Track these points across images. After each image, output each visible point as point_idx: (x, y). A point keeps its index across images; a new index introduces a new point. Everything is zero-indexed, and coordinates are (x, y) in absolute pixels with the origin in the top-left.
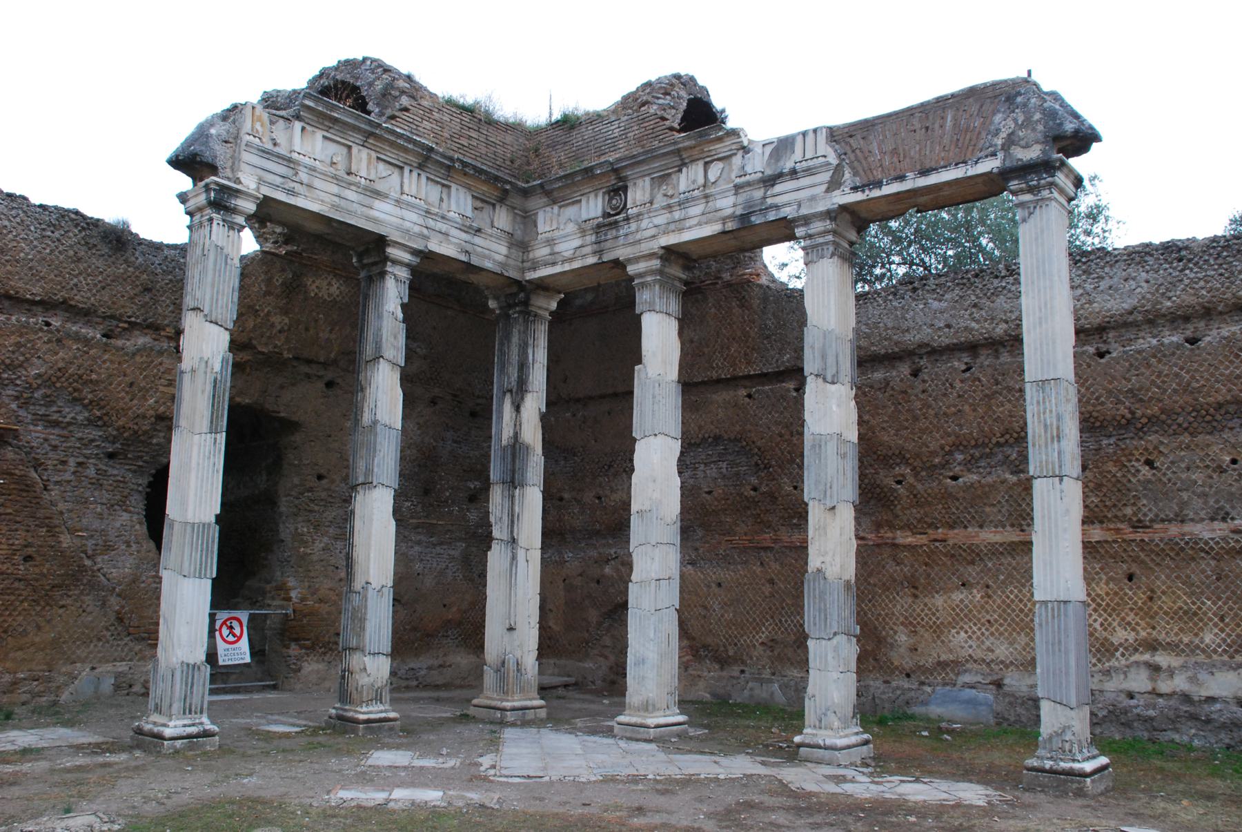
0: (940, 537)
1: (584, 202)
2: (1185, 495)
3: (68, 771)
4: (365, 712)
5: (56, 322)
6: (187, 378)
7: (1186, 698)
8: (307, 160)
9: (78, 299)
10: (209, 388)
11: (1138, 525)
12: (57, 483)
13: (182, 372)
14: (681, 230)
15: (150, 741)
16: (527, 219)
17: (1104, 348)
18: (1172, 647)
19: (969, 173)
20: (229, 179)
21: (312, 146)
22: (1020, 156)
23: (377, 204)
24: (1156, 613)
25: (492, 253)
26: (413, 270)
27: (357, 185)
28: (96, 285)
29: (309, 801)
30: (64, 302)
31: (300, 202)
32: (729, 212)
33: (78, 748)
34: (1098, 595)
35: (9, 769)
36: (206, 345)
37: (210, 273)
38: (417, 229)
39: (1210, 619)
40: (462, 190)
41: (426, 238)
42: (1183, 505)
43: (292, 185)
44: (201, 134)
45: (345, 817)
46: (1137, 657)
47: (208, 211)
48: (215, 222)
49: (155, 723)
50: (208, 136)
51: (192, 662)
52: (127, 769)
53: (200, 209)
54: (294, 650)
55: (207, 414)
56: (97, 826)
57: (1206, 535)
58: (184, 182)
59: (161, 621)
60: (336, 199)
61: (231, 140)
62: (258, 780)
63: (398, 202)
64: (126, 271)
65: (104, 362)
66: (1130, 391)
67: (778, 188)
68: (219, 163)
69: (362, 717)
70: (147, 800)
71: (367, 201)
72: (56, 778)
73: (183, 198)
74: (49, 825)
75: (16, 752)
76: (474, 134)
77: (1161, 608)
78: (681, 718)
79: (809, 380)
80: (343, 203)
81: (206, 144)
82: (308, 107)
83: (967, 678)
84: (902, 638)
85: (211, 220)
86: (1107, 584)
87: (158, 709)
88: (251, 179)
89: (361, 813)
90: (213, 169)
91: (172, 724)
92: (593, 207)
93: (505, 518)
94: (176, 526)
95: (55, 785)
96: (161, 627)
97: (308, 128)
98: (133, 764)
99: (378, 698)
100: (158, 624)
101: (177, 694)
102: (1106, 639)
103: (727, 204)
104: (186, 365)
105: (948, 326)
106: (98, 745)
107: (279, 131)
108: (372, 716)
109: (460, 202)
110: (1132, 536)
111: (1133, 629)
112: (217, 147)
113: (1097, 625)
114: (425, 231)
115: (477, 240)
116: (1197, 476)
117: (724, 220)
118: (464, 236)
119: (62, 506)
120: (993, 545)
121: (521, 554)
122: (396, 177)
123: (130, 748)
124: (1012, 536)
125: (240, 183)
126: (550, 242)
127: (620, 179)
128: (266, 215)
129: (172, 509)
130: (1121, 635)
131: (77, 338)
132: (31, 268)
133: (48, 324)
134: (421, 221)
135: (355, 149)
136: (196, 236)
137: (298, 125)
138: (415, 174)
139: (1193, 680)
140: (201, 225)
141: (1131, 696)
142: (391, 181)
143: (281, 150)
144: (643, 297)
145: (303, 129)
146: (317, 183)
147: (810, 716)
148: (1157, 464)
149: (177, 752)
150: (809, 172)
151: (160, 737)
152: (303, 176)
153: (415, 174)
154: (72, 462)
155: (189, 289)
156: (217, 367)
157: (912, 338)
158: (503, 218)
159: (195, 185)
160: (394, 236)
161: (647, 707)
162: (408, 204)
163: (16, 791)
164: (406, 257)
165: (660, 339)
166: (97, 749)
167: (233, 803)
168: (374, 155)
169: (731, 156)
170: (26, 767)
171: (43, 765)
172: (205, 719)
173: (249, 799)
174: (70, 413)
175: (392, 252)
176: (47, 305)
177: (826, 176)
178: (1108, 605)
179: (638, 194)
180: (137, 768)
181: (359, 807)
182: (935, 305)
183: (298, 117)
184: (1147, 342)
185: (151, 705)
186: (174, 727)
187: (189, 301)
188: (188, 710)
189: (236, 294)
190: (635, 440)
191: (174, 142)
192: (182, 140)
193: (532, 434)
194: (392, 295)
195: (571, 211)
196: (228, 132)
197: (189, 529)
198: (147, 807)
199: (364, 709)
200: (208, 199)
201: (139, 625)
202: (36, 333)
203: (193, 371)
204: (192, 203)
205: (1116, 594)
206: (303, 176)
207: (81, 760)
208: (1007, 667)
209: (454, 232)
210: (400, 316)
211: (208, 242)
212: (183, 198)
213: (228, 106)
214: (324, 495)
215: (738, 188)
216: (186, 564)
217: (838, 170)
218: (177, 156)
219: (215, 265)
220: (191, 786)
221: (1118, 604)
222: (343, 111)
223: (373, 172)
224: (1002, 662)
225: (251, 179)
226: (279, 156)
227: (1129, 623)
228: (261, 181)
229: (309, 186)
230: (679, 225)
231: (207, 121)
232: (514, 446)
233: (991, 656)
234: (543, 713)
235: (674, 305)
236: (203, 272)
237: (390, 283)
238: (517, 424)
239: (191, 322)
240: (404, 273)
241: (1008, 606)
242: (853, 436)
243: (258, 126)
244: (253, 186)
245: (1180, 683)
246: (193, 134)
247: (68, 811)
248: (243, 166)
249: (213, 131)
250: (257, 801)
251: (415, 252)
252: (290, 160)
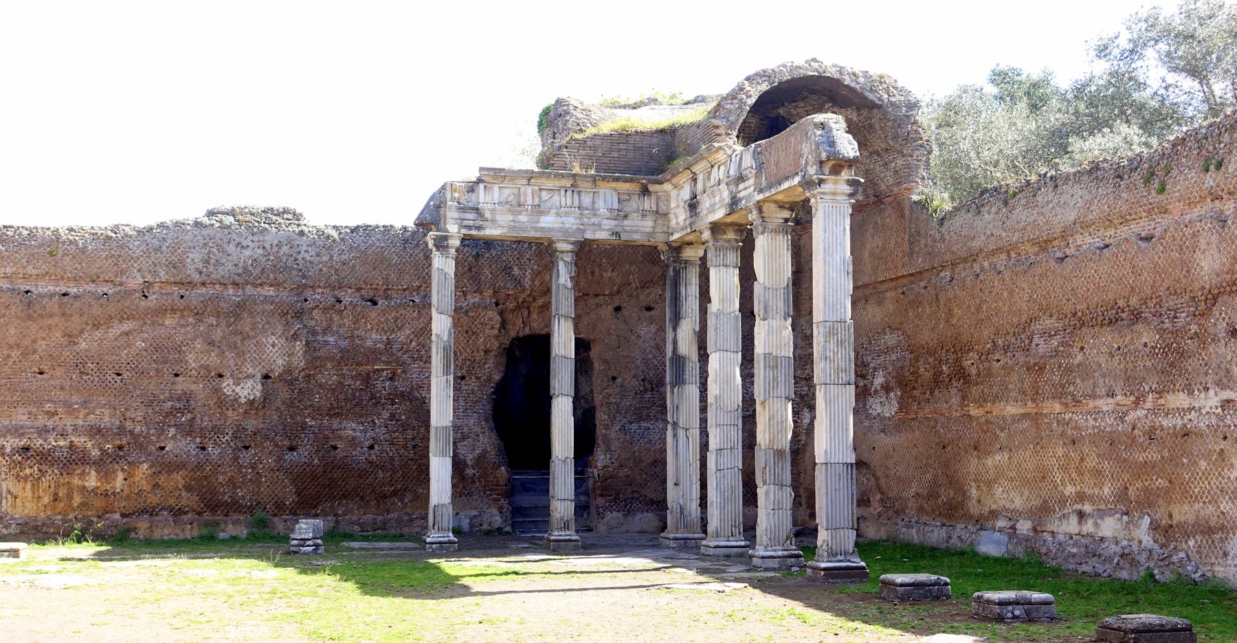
4: (556, 535)
25: (640, 229)
41: (583, 231)
71: (535, 218)
99: (566, 526)
118: (614, 222)
156: (446, 338)
164: (569, 247)
172: (451, 534)
194: (563, 276)
209: (605, 222)
210: (569, 285)
228: (461, 227)
237: (561, 265)
238: (675, 342)
240: (568, 258)
251: (574, 243)
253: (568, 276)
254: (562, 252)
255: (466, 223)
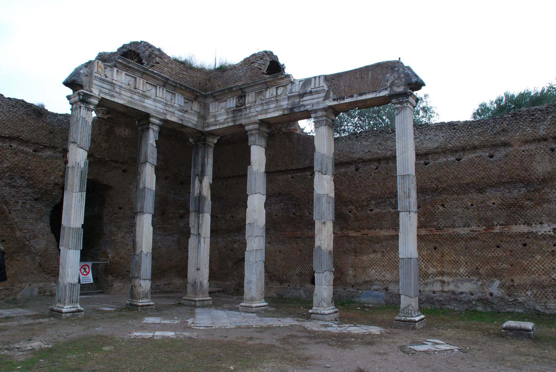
0: (365, 233)
1: (228, 101)
2: (455, 218)
3: (26, 325)
5: (14, 146)
6: (70, 171)
7: (453, 293)
8: (119, 83)
9: (23, 136)
10: (79, 174)
11: (438, 229)
12: (14, 210)
13: (68, 168)
14: (267, 113)
15: (56, 314)
16: (206, 107)
17: (427, 161)
18: (449, 274)
19: (377, 96)
20: (88, 91)
21: (121, 78)
22: (396, 90)
23: (146, 101)
24: (444, 262)
25: (192, 120)
26: (160, 127)
27: (139, 93)
28: (30, 130)
29: (123, 336)
30: (18, 137)
31: (116, 100)
32: (286, 107)
33: (28, 317)
34: (424, 255)
35: (2, 324)
36: (78, 156)
37: (80, 128)
38: (162, 111)
39: (463, 264)
40: (180, 95)
41: (165, 114)
42: (454, 221)
43: (113, 93)
44: (77, 72)
45: (138, 342)
46: (437, 278)
47: (79, 103)
48: (82, 109)
49: (58, 307)
50: (80, 73)
51: (73, 283)
52: (49, 324)
53: (76, 102)
54: (110, 278)
55: (78, 184)
56: (43, 346)
57: (462, 232)
58: (70, 92)
59: (60, 266)
60: (130, 99)
61: (89, 75)
62: (101, 329)
63: (155, 100)
64: (43, 125)
65: (34, 162)
66: (436, 178)
67: (305, 98)
68: (84, 84)
69: (140, 304)
70: (59, 336)
71: (142, 99)
72: (22, 328)
73: (69, 98)
74: (24, 345)
75: (3, 318)
76: (185, 73)
77: (446, 260)
78: (265, 304)
79: (316, 173)
80: (133, 100)
81: (79, 77)
82: (120, 62)
83: (375, 287)
84: (351, 272)
85: (80, 107)
86: (427, 251)
87: (59, 301)
88: (97, 91)
89: (143, 341)
90: (82, 87)
91: (65, 307)
92: (232, 103)
93: (196, 226)
94: (66, 229)
95: (22, 330)
96: (60, 269)
97: (120, 70)
98: (51, 322)
99: (146, 297)
100: (59, 268)
101: (67, 295)
102: (426, 272)
103: (285, 103)
104: (70, 165)
105: (370, 152)
106: (35, 315)
107: (108, 72)
108: (144, 304)
109: (179, 100)
110: (435, 233)
111: (436, 268)
112: (83, 78)
113: (423, 266)
114: (165, 111)
115: (186, 115)
116: (460, 210)
117: (284, 110)
119: (16, 220)
120: (385, 236)
121: (202, 240)
122: (154, 90)
123: (49, 317)
124: (393, 233)
125: (92, 92)
126: (215, 116)
127: (243, 92)
128: (103, 104)
129: (64, 222)
130: (431, 270)
131: (23, 152)
132: (4, 124)
133: (11, 146)
134: (163, 107)
135: (138, 79)
136: (74, 113)
137: (115, 69)
138: (161, 89)
139: (456, 286)
140: (76, 109)
141: (434, 292)
142: (152, 92)
143: (109, 79)
144: (251, 139)
145: (117, 71)
146: (123, 92)
147: (315, 302)
148: (445, 206)
149: (68, 318)
150: (317, 92)
151: (61, 312)
152: (117, 90)
153: (161, 89)
154: (20, 202)
155: (71, 134)
156: (82, 166)
157: (356, 156)
158: (196, 107)
159: (74, 93)
160: (153, 114)
161: (252, 300)
162: (159, 101)
163: (7, 333)
164: (157, 122)
165: (258, 156)
166: (35, 317)
167: (93, 337)
168: (145, 81)
169: (286, 85)
170: (9, 324)
171: (15, 323)
172: (78, 305)
173: (99, 336)
174: (19, 182)
175: (152, 119)
176: (11, 138)
177: (323, 95)
178: (427, 259)
179: (250, 98)
180: (52, 324)
181: (143, 338)
182: (365, 143)
183: (115, 66)
184: (442, 160)
185: (57, 299)
186: (66, 309)
187: (71, 139)
188: (71, 302)
189: (90, 137)
190: (247, 196)
191: (66, 74)
192: (69, 74)
193: (207, 192)
195: (223, 104)
196: (88, 72)
197: (71, 230)
198: (60, 339)
199: (141, 301)
200: (79, 98)
201: (51, 268)
202: (6, 150)
203: (73, 167)
204: (73, 100)
205: (430, 254)
206: (117, 90)
207: (30, 321)
208: (390, 283)
209: (176, 112)
210: (155, 145)
211: (79, 116)
212: (69, 98)
213: (87, 61)
214: (122, 215)
215: (289, 98)
216: (70, 244)
217: (328, 92)
218: (67, 81)
219: (82, 125)
220: (76, 331)
221: (431, 258)
222: (133, 64)
223: (145, 88)
224: (388, 281)
225: (97, 91)
226: (107, 81)
227: (434, 266)
228: (100, 91)
229: (120, 94)
230: (266, 111)
231: (79, 67)
232: (199, 197)
233: (384, 279)
234: (211, 302)
235: (263, 143)
236: (77, 127)
237: (151, 132)
238: (201, 188)
239: (72, 148)
240: (156, 128)
241: (391, 260)
242: (332, 195)
243: (100, 70)
244: (97, 93)
245: (451, 287)
246: (73, 73)
247: (30, 340)
248: (93, 85)
249: (82, 71)
250: (103, 336)
251: (161, 120)
252: (112, 83)
253: (154, 139)
254: (153, 124)
255: (104, 90)
